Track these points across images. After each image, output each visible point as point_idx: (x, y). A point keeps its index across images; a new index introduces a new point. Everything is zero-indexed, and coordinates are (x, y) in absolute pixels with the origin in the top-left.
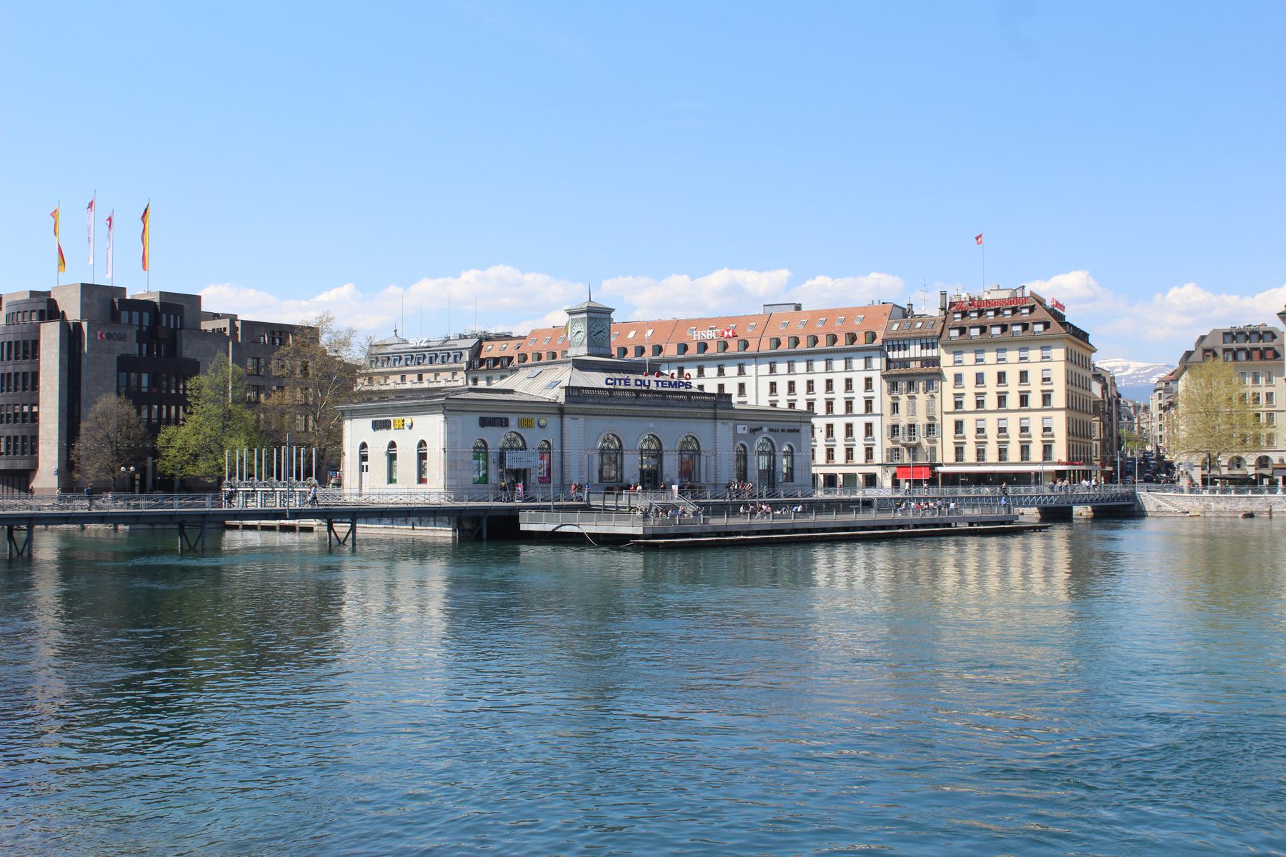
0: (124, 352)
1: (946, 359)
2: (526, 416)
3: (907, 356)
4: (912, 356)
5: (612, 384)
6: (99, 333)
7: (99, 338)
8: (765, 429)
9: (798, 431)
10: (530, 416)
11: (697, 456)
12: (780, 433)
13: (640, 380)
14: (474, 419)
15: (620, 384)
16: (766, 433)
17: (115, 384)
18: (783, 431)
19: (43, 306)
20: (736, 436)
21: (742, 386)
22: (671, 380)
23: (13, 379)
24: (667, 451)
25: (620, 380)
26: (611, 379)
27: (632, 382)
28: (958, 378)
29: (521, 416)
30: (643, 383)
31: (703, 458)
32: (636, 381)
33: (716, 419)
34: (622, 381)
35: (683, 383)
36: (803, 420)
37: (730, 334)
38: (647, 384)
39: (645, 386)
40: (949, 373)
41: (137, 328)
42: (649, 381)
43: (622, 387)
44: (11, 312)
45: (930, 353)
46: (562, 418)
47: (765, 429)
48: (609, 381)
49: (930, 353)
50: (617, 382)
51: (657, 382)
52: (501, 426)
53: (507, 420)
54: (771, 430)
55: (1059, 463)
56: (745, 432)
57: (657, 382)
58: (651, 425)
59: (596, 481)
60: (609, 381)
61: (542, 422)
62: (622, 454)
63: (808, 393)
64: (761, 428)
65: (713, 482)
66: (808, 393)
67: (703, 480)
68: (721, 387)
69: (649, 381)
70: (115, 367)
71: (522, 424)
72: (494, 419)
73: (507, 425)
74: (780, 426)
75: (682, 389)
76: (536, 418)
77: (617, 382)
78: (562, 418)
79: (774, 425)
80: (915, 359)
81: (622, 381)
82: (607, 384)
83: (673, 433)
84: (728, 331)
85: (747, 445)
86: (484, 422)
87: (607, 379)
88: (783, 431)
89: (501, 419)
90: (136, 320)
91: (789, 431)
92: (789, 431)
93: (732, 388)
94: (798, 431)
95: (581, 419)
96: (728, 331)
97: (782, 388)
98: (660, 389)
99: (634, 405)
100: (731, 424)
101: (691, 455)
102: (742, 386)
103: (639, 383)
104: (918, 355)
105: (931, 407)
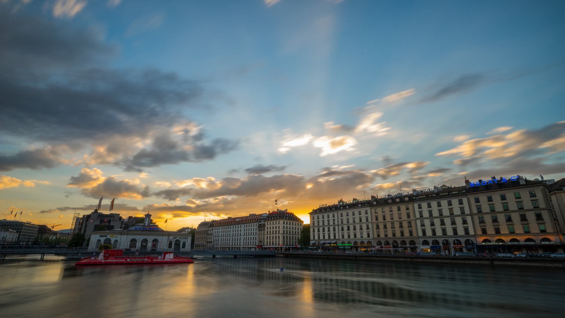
8: (178, 238)
9: (188, 238)
14: (99, 235)
18: (183, 238)
28: (268, 227)
31: (159, 244)
40: (266, 226)
43: (139, 229)
45: (264, 223)
47: (178, 238)
49: (264, 223)
53: (107, 236)
54: (179, 238)
55: (282, 245)
61: (116, 236)
64: (177, 238)
67: (158, 248)
71: (111, 237)
74: (182, 237)
79: (181, 237)
80: (262, 224)
83: (150, 238)
86: (101, 236)
88: (183, 238)
89: (105, 236)
91: (185, 238)
92: (185, 238)
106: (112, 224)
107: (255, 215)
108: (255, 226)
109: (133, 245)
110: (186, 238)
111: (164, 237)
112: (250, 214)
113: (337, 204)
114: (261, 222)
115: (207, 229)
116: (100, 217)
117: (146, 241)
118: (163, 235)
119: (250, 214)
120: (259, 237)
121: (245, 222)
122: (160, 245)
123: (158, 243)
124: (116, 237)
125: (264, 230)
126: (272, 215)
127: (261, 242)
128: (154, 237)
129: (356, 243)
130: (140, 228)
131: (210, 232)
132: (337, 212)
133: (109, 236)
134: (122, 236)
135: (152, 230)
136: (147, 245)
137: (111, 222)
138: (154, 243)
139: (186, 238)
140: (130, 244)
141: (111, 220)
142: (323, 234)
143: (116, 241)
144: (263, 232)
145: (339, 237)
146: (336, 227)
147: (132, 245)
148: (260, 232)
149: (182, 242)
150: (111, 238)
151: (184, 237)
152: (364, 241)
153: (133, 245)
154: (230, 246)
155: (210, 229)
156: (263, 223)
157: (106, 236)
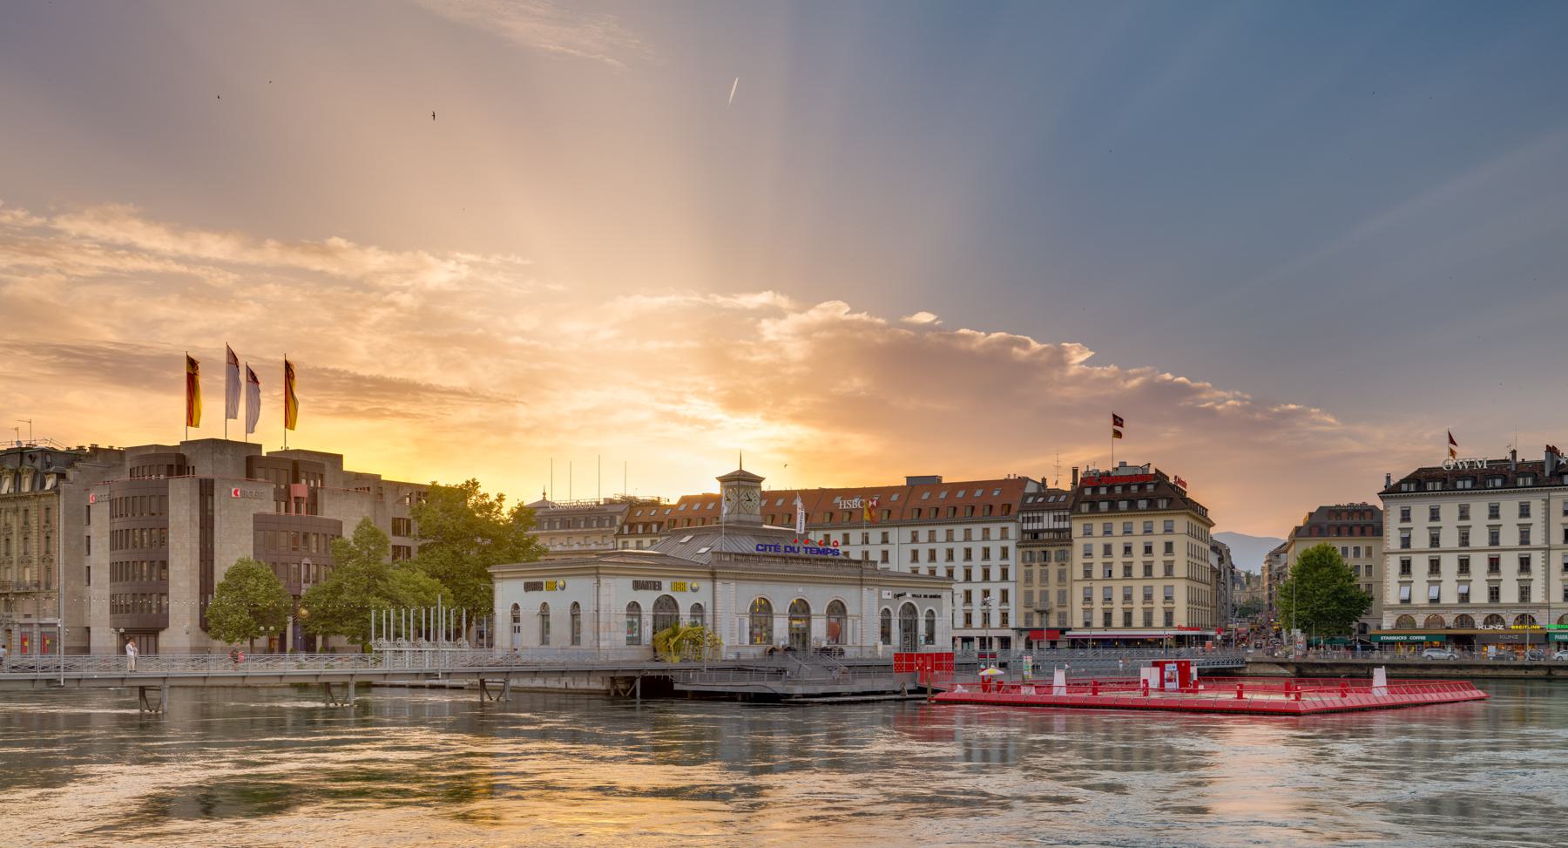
1: (1077, 528)
2: (678, 581)
3: (1040, 527)
4: (1046, 527)
6: (233, 490)
7: (233, 495)
9: (940, 597)
10: (682, 581)
11: (844, 620)
12: (923, 598)
13: (790, 547)
14: (629, 582)
15: (770, 550)
18: (925, 596)
19: (173, 462)
20: (881, 601)
21: (885, 553)
22: (819, 546)
23: (119, 534)
24: (814, 615)
25: (770, 546)
26: (762, 545)
27: (782, 549)
29: (674, 580)
30: (792, 549)
31: (849, 621)
32: (786, 547)
33: (862, 585)
34: (773, 548)
35: (831, 550)
36: (944, 586)
37: (875, 503)
38: (796, 549)
39: (794, 551)
42: (798, 548)
43: (772, 553)
44: (135, 466)
46: (714, 582)
47: (909, 595)
48: (760, 547)
50: (768, 548)
52: (655, 589)
53: (660, 583)
54: (914, 596)
56: (890, 597)
57: (806, 548)
58: (800, 590)
59: (747, 642)
60: (760, 547)
61: (695, 585)
62: (772, 617)
63: (947, 561)
64: (905, 594)
65: (859, 644)
66: (947, 561)
67: (849, 642)
68: (866, 554)
69: (798, 548)
70: (251, 525)
71: (676, 587)
72: (647, 582)
73: (660, 589)
74: (923, 592)
75: (830, 556)
76: (689, 583)
77: (768, 548)
78: (714, 582)
80: (1048, 531)
81: (773, 548)
82: (757, 549)
83: (819, 598)
84: (873, 501)
85: (891, 609)
86: (638, 586)
88: (925, 596)
91: (931, 597)
92: (931, 597)
93: (875, 556)
94: (940, 597)
96: (873, 501)
97: (924, 556)
98: (809, 555)
99: (784, 571)
100: (876, 590)
101: (838, 619)
102: (885, 553)
103: (788, 549)
104: (1051, 527)
105: (1063, 576)
107: (933, 482)
108: (1002, 538)
109: (761, 627)
110: (935, 597)
112: (908, 478)
113: (1543, 458)
114: (1039, 520)
117: (800, 609)
119: (908, 478)
120: (1029, 595)
121: (885, 517)
123: (846, 618)
124: (695, 590)
125: (1064, 558)
126: (1103, 491)
127: (1043, 613)
129: (1464, 620)
130: (777, 548)
131: (282, 548)
132: (1545, 496)
133: (667, 589)
134: (865, 589)
136: (809, 627)
138: (833, 620)
139: (935, 597)
140: (752, 627)
141: (316, 487)
142: (1431, 583)
143: (697, 609)
144: (1053, 568)
145: (1547, 595)
146: (1537, 560)
147: (757, 630)
148: (1036, 568)
149: (922, 614)
150: (675, 596)
151: (929, 593)
152: (1503, 614)
153: (761, 627)
154: (991, 633)
156: (1048, 521)
157: (657, 586)
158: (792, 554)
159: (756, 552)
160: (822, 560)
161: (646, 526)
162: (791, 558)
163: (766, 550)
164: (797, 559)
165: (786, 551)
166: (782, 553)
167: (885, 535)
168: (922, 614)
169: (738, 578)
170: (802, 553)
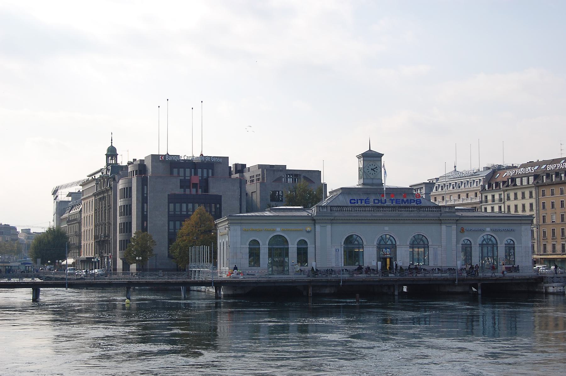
0: (173, 192)
5: (355, 203)
15: (361, 203)
16: (488, 231)
17: (167, 210)
25: (361, 200)
26: (355, 200)
32: (374, 200)
33: (441, 223)
34: (363, 201)
41: (200, 178)
50: (359, 201)
51: (392, 200)
54: (493, 230)
58: (387, 228)
77: (359, 201)
81: (363, 201)
82: (351, 203)
87: (351, 200)
90: (182, 173)
95: (329, 227)
106: (213, 191)
111: (444, 227)
115: (478, 200)
116: (175, 171)
118: (440, 221)
122: (435, 255)
128: (412, 231)
135: (403, 204)
137: (211, 184)
149: (501, 244)
155: (490, 198)
158: (379, 204)
159: (350, 205)
160: (405, 207)
161: (497, 184)
162: (378, 207)
163: (357, 203)
164: (383, 207)
165: (374, 203)
166: (372, 204)
167: (332, 189)
168: (501, 244)
169: (333, 221)
170: (388, 203)
